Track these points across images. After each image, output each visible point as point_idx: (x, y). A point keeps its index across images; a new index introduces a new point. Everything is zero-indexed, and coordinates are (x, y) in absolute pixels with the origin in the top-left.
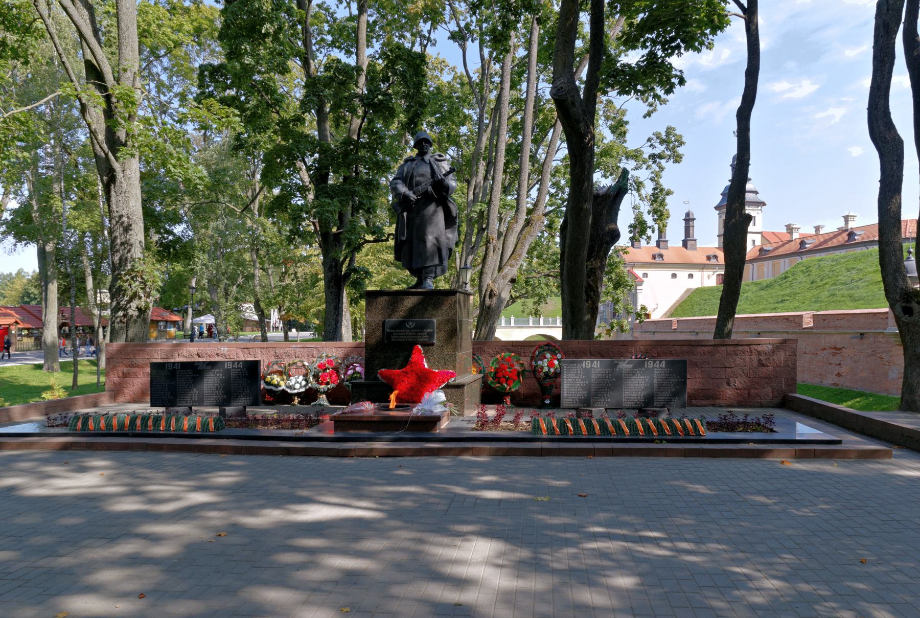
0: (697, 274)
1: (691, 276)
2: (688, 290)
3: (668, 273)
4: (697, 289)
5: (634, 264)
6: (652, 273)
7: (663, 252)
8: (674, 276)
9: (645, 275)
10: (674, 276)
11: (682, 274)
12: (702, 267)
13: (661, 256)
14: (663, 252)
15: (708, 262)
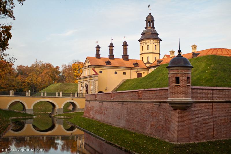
0: (128, 72)
1: (124, 73)
2: (123, 80)
3: (112, 71)
4: (127, 80)
5: (95, 66)
6: (104, 70)
7: (110, 60)
8: (116, 73)
9: (101, 72)
10: (116, 73)
11: (120, 72)
12: (131, 68)
13: (108, 63)
14: (111, 61)
15: (134, 67)
